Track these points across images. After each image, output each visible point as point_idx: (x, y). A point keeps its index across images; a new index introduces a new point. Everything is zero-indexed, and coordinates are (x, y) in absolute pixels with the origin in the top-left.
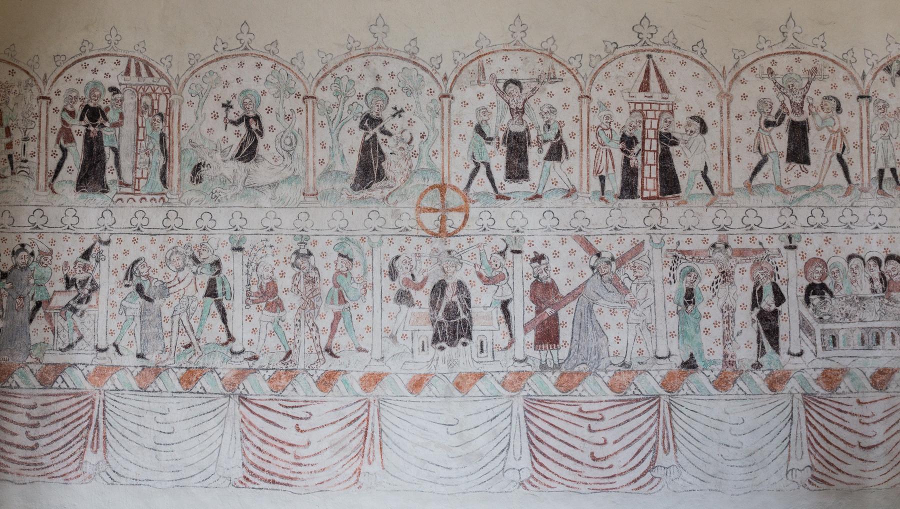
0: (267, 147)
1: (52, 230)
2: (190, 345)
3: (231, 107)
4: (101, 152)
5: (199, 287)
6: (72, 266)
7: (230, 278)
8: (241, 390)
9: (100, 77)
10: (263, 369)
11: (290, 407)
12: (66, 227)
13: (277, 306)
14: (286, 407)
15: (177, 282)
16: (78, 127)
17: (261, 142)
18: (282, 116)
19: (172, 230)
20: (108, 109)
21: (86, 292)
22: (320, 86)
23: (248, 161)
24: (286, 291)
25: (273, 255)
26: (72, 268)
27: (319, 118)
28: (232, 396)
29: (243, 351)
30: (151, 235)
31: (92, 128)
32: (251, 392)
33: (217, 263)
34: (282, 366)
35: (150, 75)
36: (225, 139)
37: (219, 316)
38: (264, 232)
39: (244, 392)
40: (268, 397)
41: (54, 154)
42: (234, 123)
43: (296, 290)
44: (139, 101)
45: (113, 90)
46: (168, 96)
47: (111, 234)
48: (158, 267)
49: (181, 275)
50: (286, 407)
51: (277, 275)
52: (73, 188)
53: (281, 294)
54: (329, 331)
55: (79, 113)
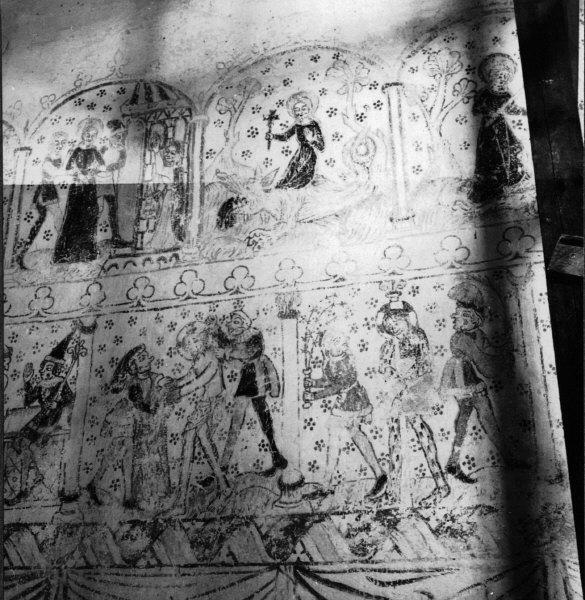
0: (330, 162)
1: (16, 320)
2: (209, 480)
3: (277, 118)
5: (226, 380)
6: (37, 367)
7: (277, 362)
8: (298, 554)
10: (338, 514)
11: (389, 583)
12: (35, 313)
13: (358, 399)
14: (382, 584)
15: (193, 376)
17: (321, 157)
18: (352, 115)
19: (189, 298)
20: (104, 150)
21: (54, 405)
22: (407, 68)
23: (304, 185)
24: (369, 373)
25: (347, 317)
26: (37, 372)
27: (406, 111)
28: (282, 567)
29: (301, 483)
30: (155, 309)
32: (317, 557)
33: (257, 341)
34: (370, 504)
36: (267, 162)
37: (258, 425)
38: (331, 283)
39: (304, 558)
40: (346, 567)
42: (281, 138)
43: (389, 370)
46: (188, 118)
47: (98, 316)
48: (165, 357)
49: (200, 365)
50: (382, 584)
51: (354, 349)
52: (49, 257)
53: (362, 379)
54: (453, 434)
55: (65, 161)
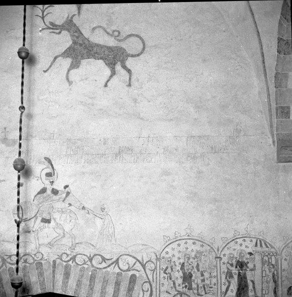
4: (246, 282)
9: (243, 247)
16: (235, 271)
20: (248, 263)
31: (241, 271)
35: (267, 247)
41: (225, 284)
44: (262, 259)
45: (251, 254)
55: (235, 264)
